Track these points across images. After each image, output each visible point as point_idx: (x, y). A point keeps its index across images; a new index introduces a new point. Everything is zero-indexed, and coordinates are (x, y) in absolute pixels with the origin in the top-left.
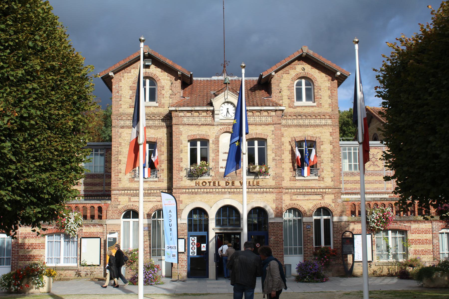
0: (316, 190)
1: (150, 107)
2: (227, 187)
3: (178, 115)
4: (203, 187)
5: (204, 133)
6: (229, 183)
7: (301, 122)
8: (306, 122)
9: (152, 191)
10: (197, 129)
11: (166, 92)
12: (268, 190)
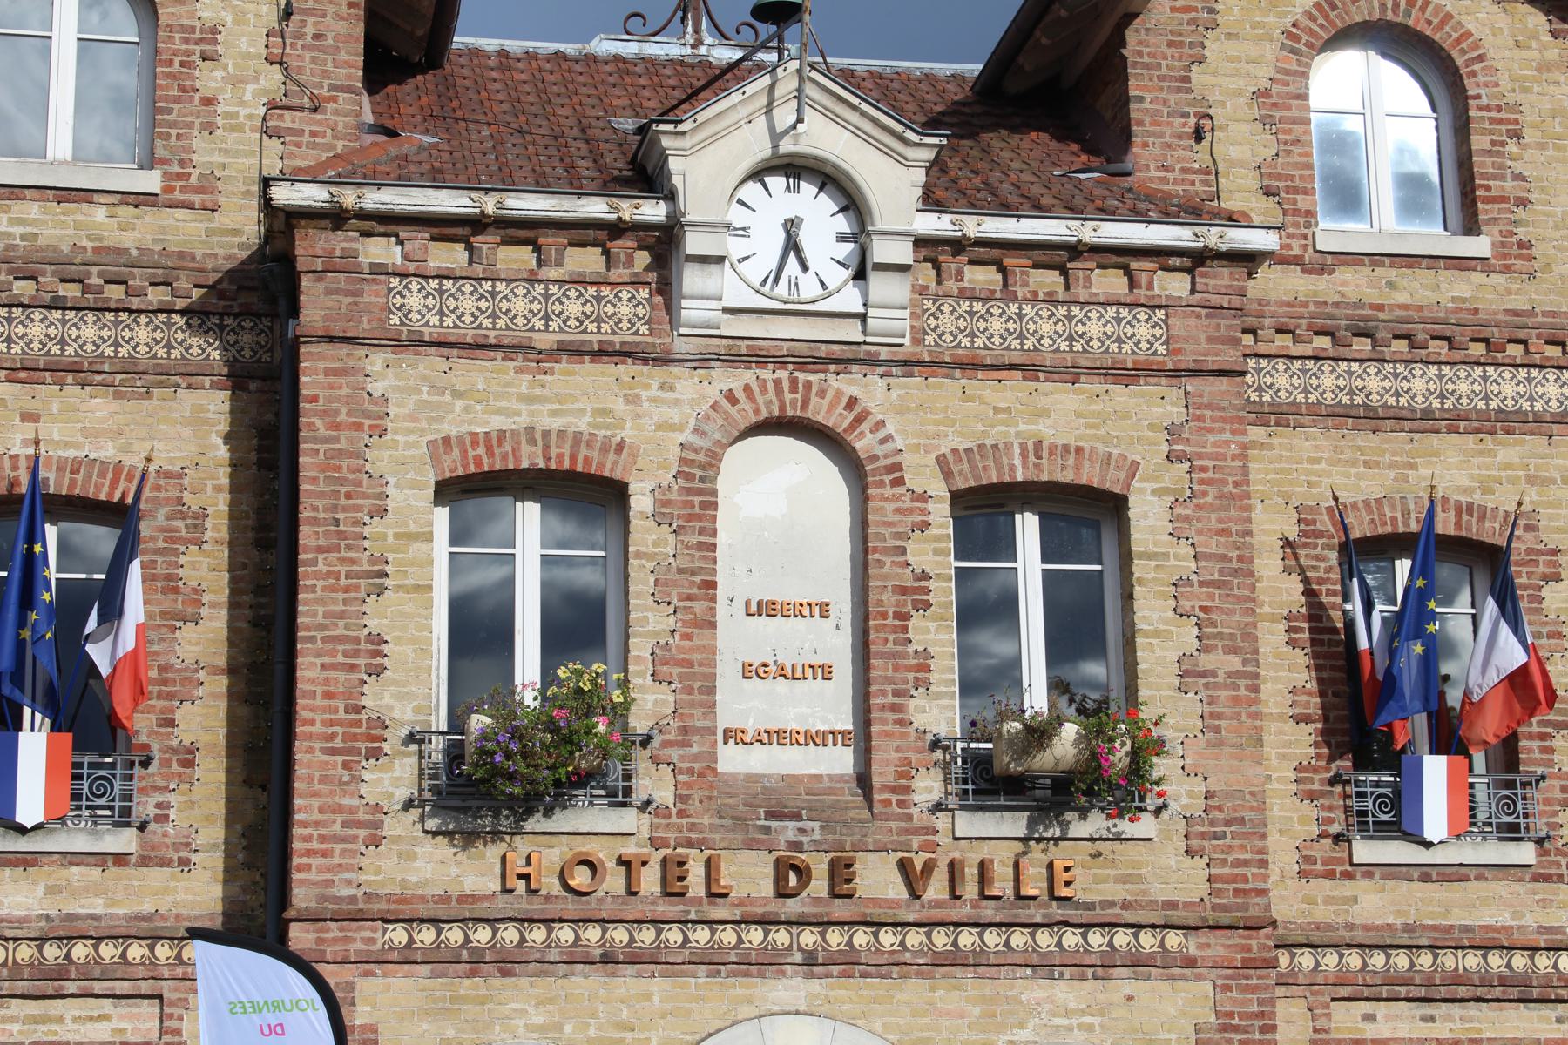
0: (1519, 961)
1: (86, 195)
2: (792, 907)
3: (352, 255)
4: (572, 907)
5: (583, 424)
6: (804, 873)
7: (1375, 383)
8: (1418, 385)
9: (80, 951)
10: (524, 383)
11: (237, 82)
12: (1147, 940)
